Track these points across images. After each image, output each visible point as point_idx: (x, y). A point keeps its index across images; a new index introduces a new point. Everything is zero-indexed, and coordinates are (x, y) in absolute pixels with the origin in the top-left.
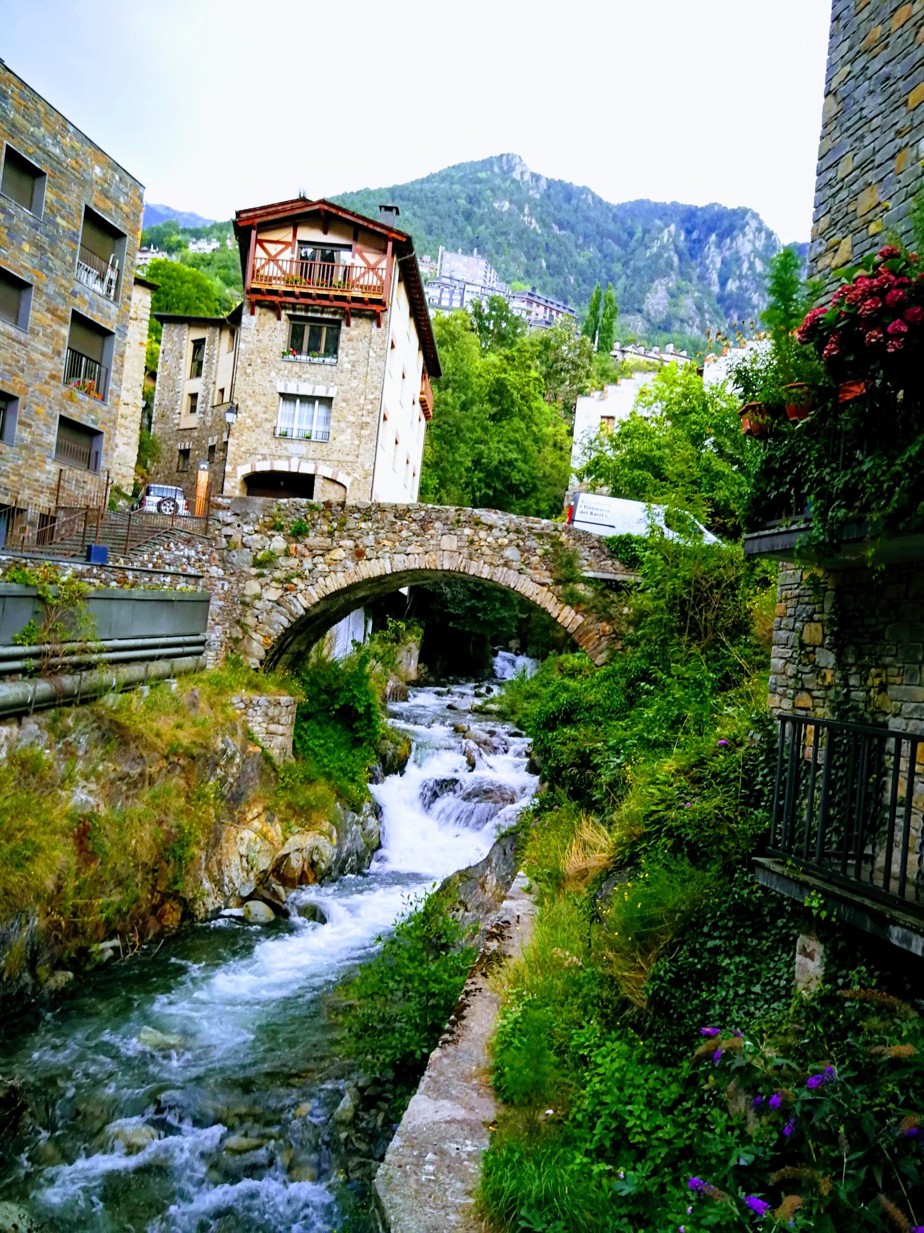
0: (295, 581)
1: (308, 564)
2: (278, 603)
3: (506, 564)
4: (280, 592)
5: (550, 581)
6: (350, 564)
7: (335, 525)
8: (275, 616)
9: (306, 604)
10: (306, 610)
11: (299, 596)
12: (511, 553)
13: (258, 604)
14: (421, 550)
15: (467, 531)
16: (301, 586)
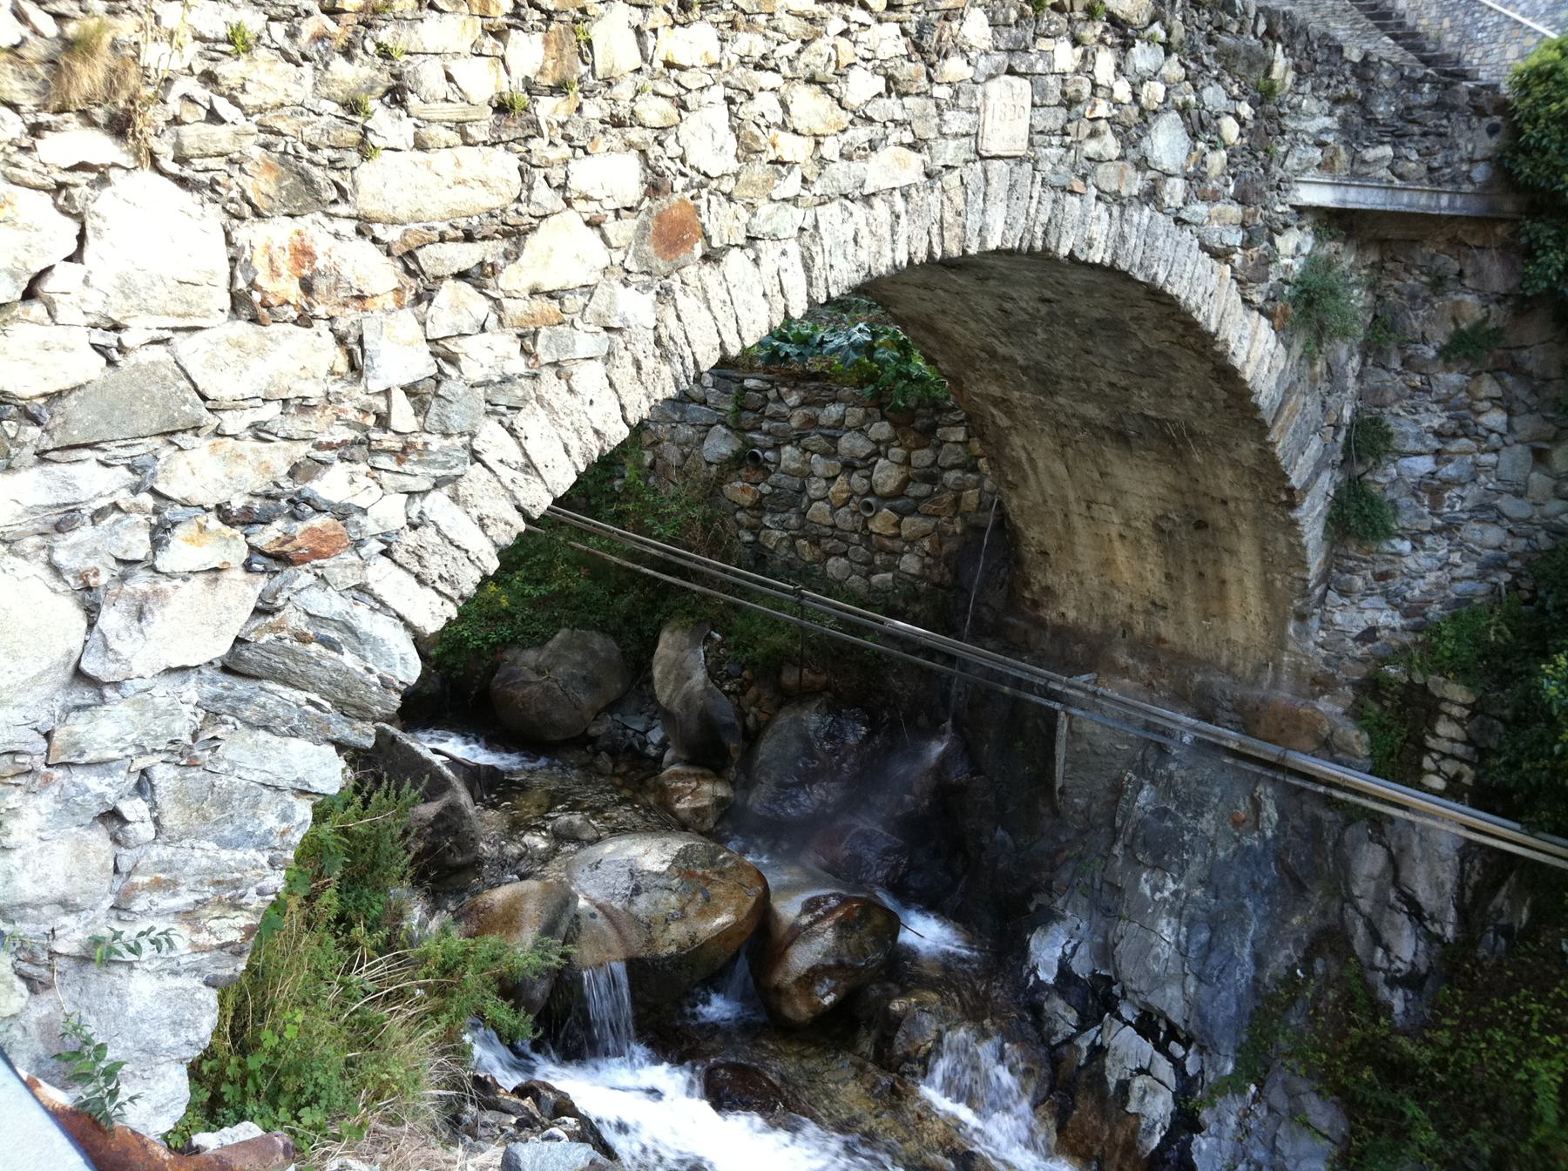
0: (333, 485)
1: (399, 356)
2: (234, 665)
3: (1151, 195)
4: (243, 591)
5: (1235, 238)
6: (636, 307)
7: (528, 53)
8: (249, 757)
9: (433, 614)
10: (419, 640)
11: (386, 579)
12: (1167, 143)
13: (105, 730)
14: (910, 168)
15: (1065, 56)
16: (388, 512)
